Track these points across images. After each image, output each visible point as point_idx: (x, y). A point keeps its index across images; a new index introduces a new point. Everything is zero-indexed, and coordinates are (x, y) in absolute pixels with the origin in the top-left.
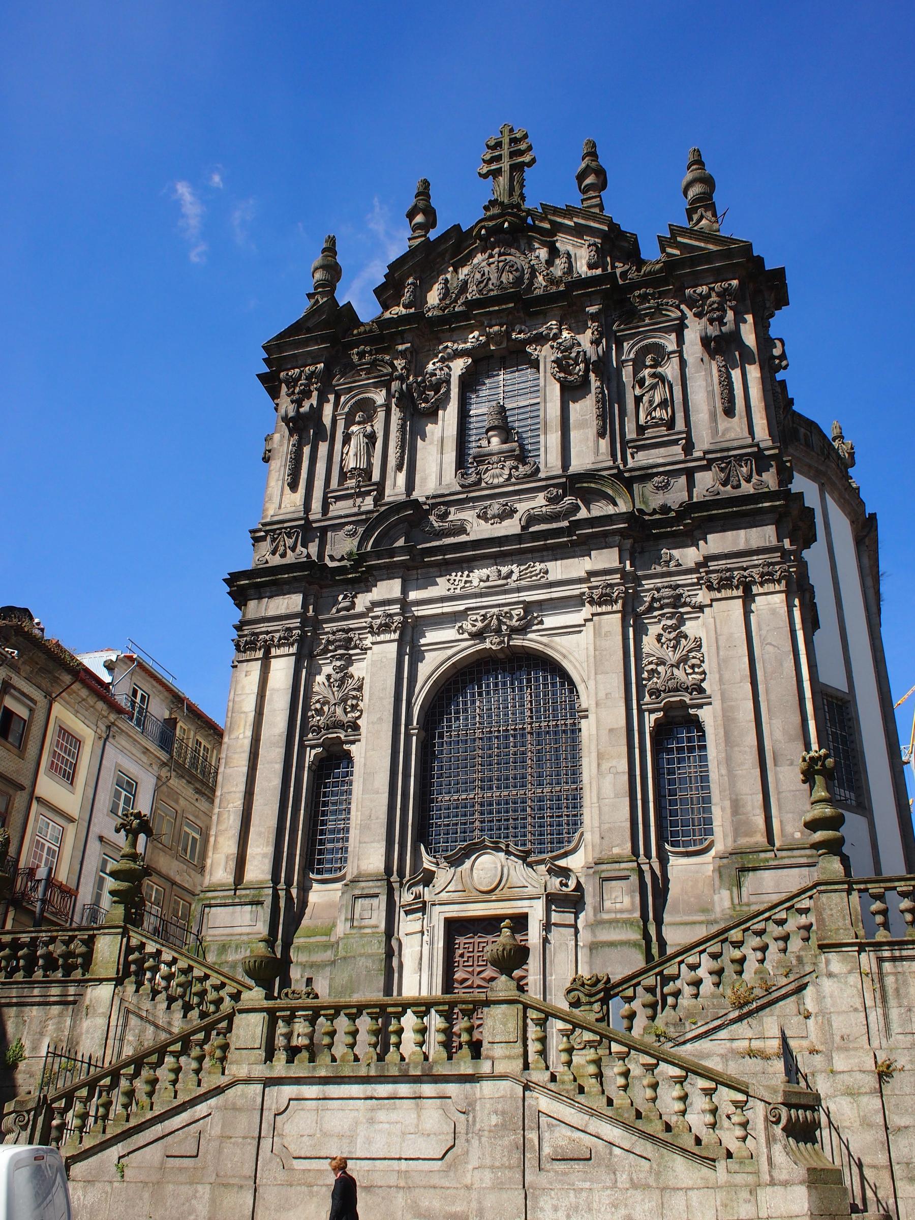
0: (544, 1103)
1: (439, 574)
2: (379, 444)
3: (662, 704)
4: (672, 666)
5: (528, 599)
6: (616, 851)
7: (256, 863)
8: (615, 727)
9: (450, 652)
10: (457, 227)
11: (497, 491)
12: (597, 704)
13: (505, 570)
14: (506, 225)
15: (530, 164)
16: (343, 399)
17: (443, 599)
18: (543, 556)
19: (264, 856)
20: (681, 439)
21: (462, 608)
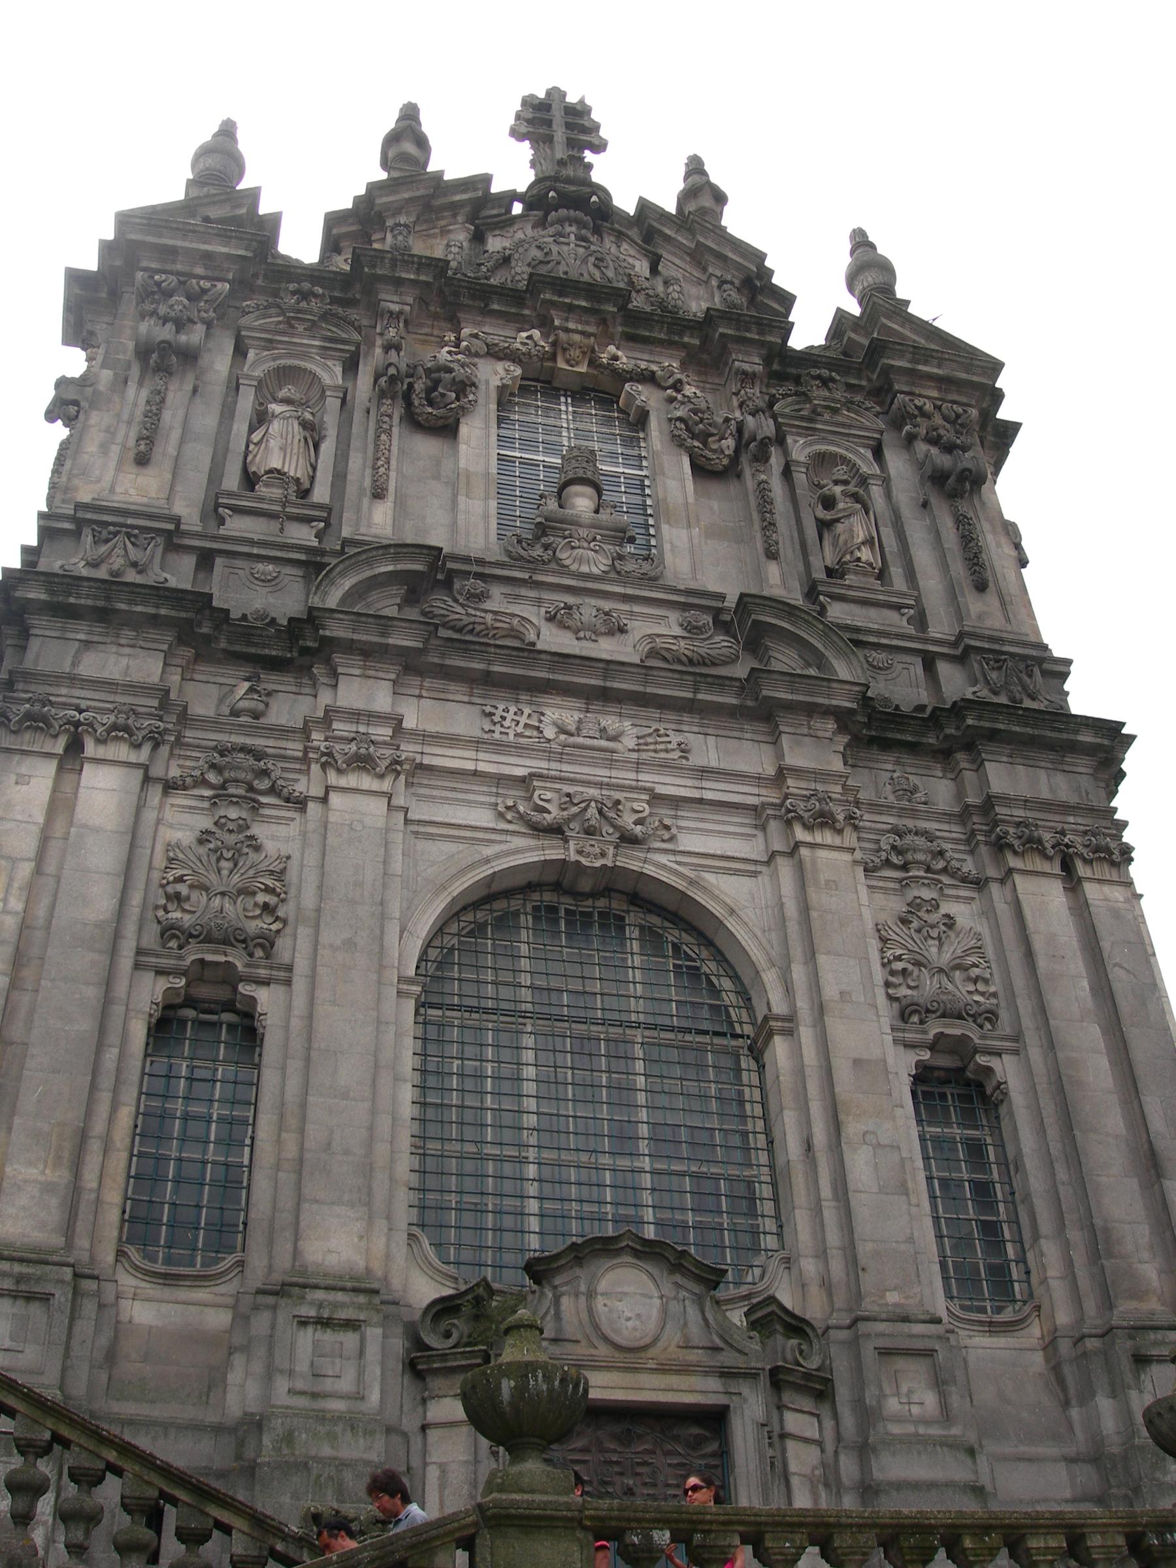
1: (466, 699)
2: (328, 448)
3: (931, 1036)
4: (941, 970)
5: (660, 790)
6: (892, 1297)
7: (23, 1200)
8: (865, 1056)
9: (489, 851)
10: (486, 179)
11: (590, 585)
12: (820, 1010)
13: (610, 722)
16: (251, 354)
17: (477, 744)
18: (680, 722)
19: (48, 1188)
21: (520, 772)
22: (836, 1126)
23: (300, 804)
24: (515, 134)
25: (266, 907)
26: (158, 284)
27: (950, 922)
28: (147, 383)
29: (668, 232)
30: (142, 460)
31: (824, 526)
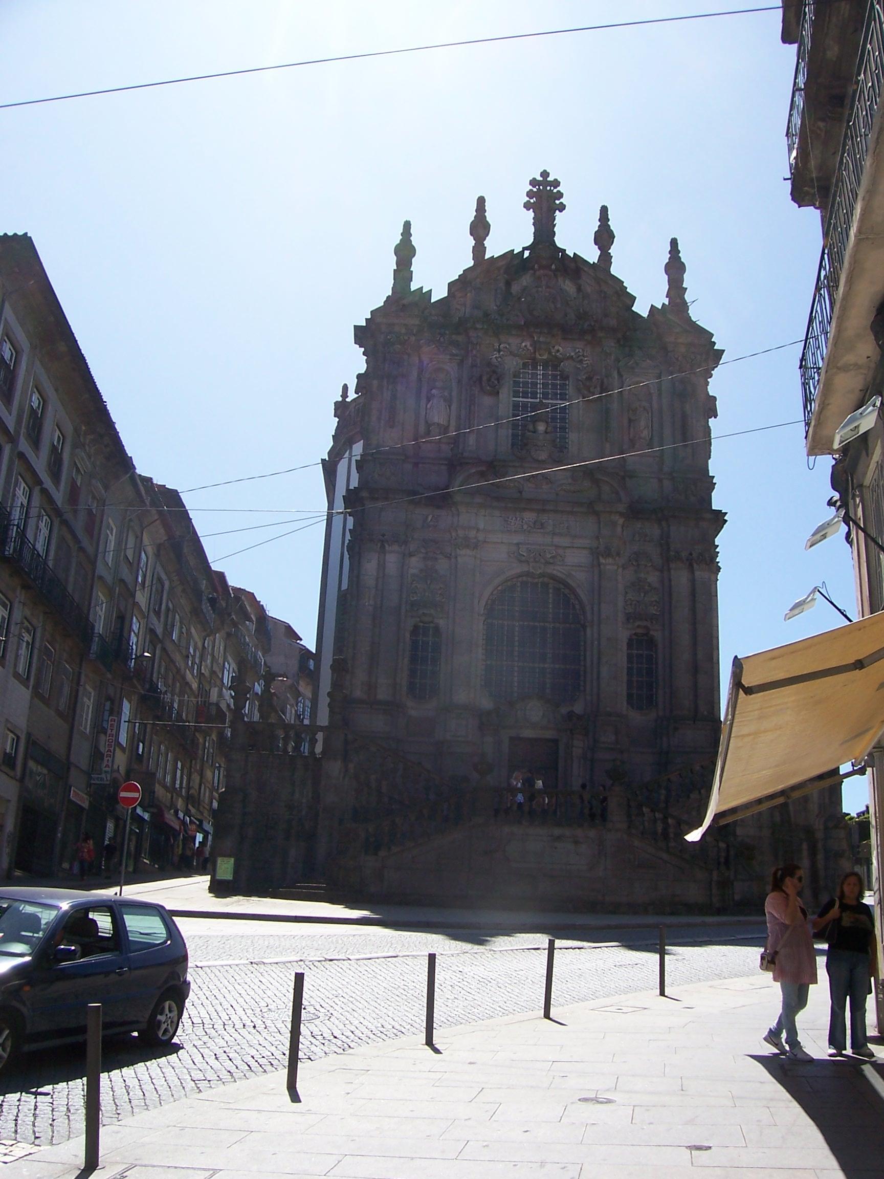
0: (636, 843)
2: (454, 407)
6: (608, 709)
14: (553, 267)
15: (561, 211)
20: (657, 456)
21: (515, 542)
22: (599, 659)
23: (449, 557)
24: (527, 206)
25: (440, 594)
26: (390, 340)
27: (650, 585)
28: (390, 387)
29: (586, 269)
30: (392, 427)
31: (630, 421)
